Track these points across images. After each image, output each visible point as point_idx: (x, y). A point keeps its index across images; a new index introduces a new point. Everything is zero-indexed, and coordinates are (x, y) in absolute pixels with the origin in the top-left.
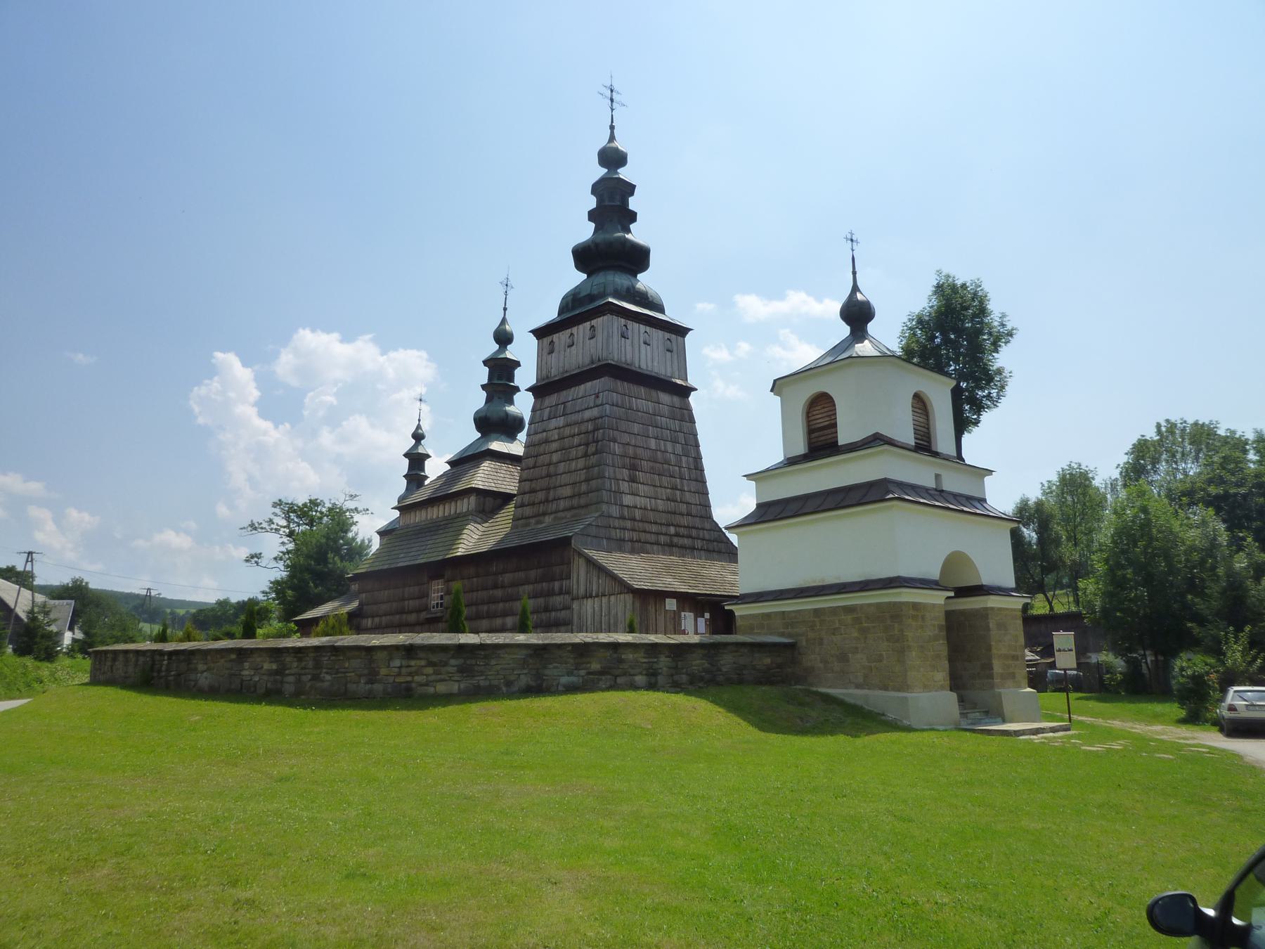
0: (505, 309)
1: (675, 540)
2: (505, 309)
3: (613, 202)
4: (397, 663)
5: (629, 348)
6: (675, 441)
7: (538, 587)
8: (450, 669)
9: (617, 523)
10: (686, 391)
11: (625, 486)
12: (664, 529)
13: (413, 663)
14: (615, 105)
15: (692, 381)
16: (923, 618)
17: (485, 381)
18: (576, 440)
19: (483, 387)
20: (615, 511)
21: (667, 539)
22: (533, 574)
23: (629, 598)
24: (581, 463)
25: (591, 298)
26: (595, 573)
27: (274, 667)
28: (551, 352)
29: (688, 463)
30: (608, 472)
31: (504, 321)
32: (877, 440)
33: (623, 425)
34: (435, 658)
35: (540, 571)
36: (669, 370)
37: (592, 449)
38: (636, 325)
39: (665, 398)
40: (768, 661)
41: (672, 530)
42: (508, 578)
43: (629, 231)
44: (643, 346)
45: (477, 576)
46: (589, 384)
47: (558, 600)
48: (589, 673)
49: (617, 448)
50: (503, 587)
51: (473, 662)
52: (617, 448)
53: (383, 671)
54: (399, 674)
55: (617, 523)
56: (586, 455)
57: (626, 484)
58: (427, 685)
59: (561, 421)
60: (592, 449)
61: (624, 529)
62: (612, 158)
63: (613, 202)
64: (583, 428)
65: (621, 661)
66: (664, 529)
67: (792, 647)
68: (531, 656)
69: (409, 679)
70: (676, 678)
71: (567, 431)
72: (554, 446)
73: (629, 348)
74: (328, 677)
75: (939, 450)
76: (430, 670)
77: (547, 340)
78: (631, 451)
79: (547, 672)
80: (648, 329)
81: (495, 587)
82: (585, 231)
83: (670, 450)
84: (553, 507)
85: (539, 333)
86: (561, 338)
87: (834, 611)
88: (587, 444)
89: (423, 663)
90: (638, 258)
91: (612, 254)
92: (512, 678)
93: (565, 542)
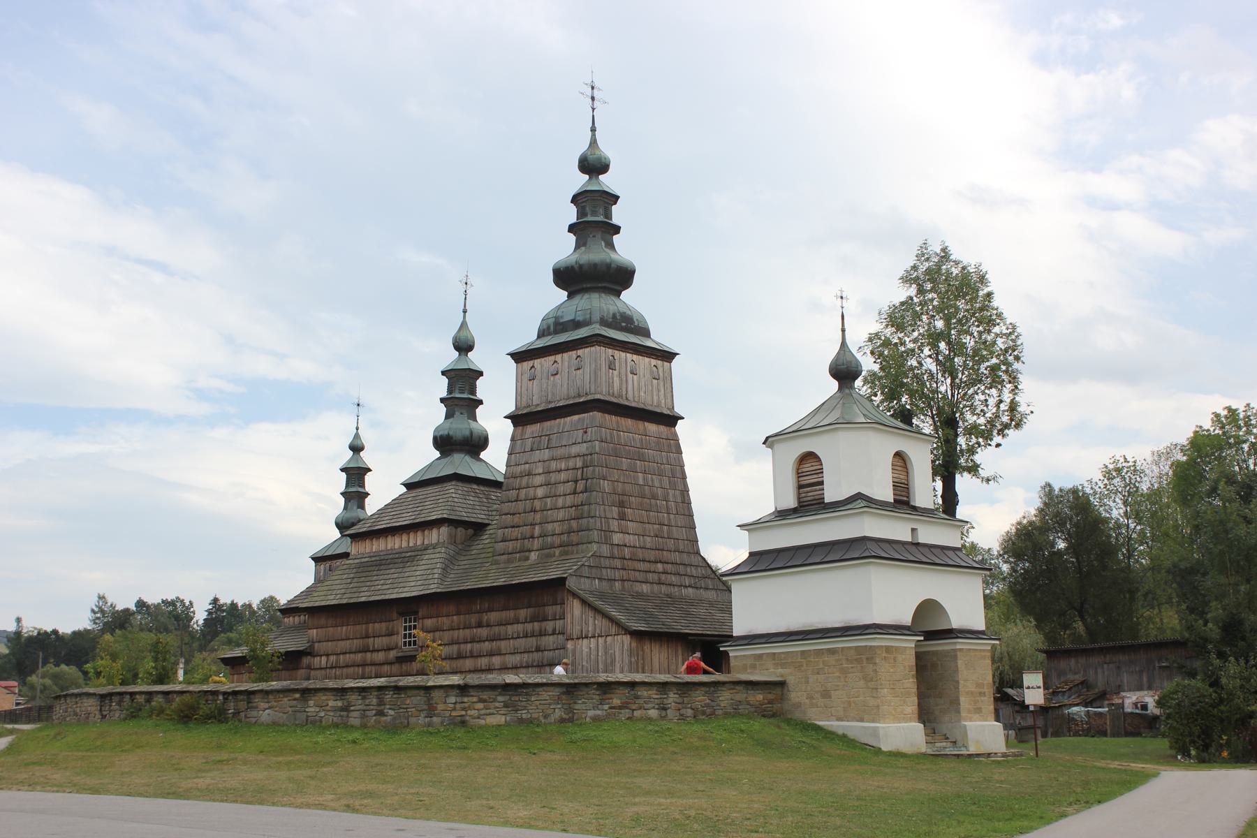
0: (465, 312)
1: (663, 577)
2: (465, 312)
3: (594, 214)
5: (616, 380)
6: (661, 474)
7: (529, 627)
9: (607, 563)
10: (671, 420)
11: (614, 525)
12: (652, 567)
15: (678, 410)
17: (444, 394)
18: (563, 476)
19: (442, 400)
20: (605, 550)
21: (655, 576)
22: (523, 613)
23: (627, 638)
24: (569, 500)
25: (576, 325)
26: (591, 614)
28: (532, 379)
29: (674, 496)
30: (598, 510)
31: (464, 325)
32: (860, 502)
36: (655, 398)
37: (581, 485)
38: (623, 354)
39: (652, 428)
41: (660, 566)
42: (494, 616)
43: (611, 246)
44: (630, 376)
45: (458, 614)
46: (576, 417)
47: (549, 641)
49: (606, 485)
52: (606, 485)
55: (607, 563)
57: (616, 523)
59: (546, 454)
60: (581, 485)
62: (593, 166)
63: (594, 214)
64: (571, 464)
65: (637, 697)
66: (652, 567)
67: (782, 684)
68: (564, 693)
70: (683, 711)
71: (554, 465)
72: (538, 480)
73: (616, 380)
76: (481, 705)
77: (527, 365)
78: (620, 487)
80: (635, 357)
82: (564, 248)
85: (519, 357)
87: (819, 653)
88: (576, 481)
90: (621, 277)
91: (594, 275)
92: (549, 711)
93: (561, 582)
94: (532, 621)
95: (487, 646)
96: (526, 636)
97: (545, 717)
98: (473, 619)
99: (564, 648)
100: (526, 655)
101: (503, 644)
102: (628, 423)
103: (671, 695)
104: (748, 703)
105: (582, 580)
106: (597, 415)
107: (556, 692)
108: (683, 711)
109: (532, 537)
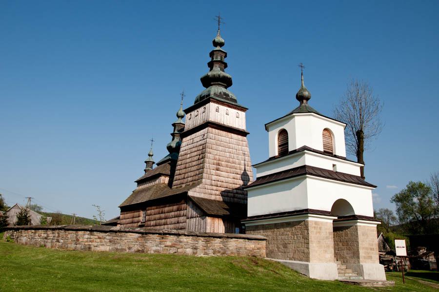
4: (87, 236)
5: (219, 117)
7: (176, 213)
8: (106, 240)
13: (92, 237)
14: (220, 23)
16: (320, 228)
22: (175, 207)
27: (45, 235)
33: (214, 146)
34: (101, 235)
35: (177, 206)
40: (253, 246)
42: (166, 209)
46: (202, 131)
47: (181, 219)
48: (165, 246)
49: (211, 156)
50: (165, 213)
51: (116, 238)
52: (211, 156)
53: (81, 240)
54: (87, 242)
56: (199, 159)
57: (214, 171)
58: (97, 246)
60: (201, 157)
61: (212, 190)
65: (181, 242)
68: (140, 237)
69: (90, 243)
70: (206, 251)
74: (62, 241)
75: (337, 154)
76: (99, 240)
79: (146, 244)
80: (229, 108)
81: (162, 213)
83: (235, 157)
84: (185, 180)
86: (194, 113)
88: (199, 155)
89: (96, 237)
92: (132, 246)
94: (177, 211)
95: (163, 221)
96: (175, 217)
97: (130, 248)
98: (161, 210)
99: (185, 222)
100: (174, 225)
101: (168, 220)
102: (224, 133)
103: (200, 242)
104: (246, 249)
105: (195, 193)
106: (210, 129)
107: (137, 235)
108: (206, 251)
109: (184, 178)
